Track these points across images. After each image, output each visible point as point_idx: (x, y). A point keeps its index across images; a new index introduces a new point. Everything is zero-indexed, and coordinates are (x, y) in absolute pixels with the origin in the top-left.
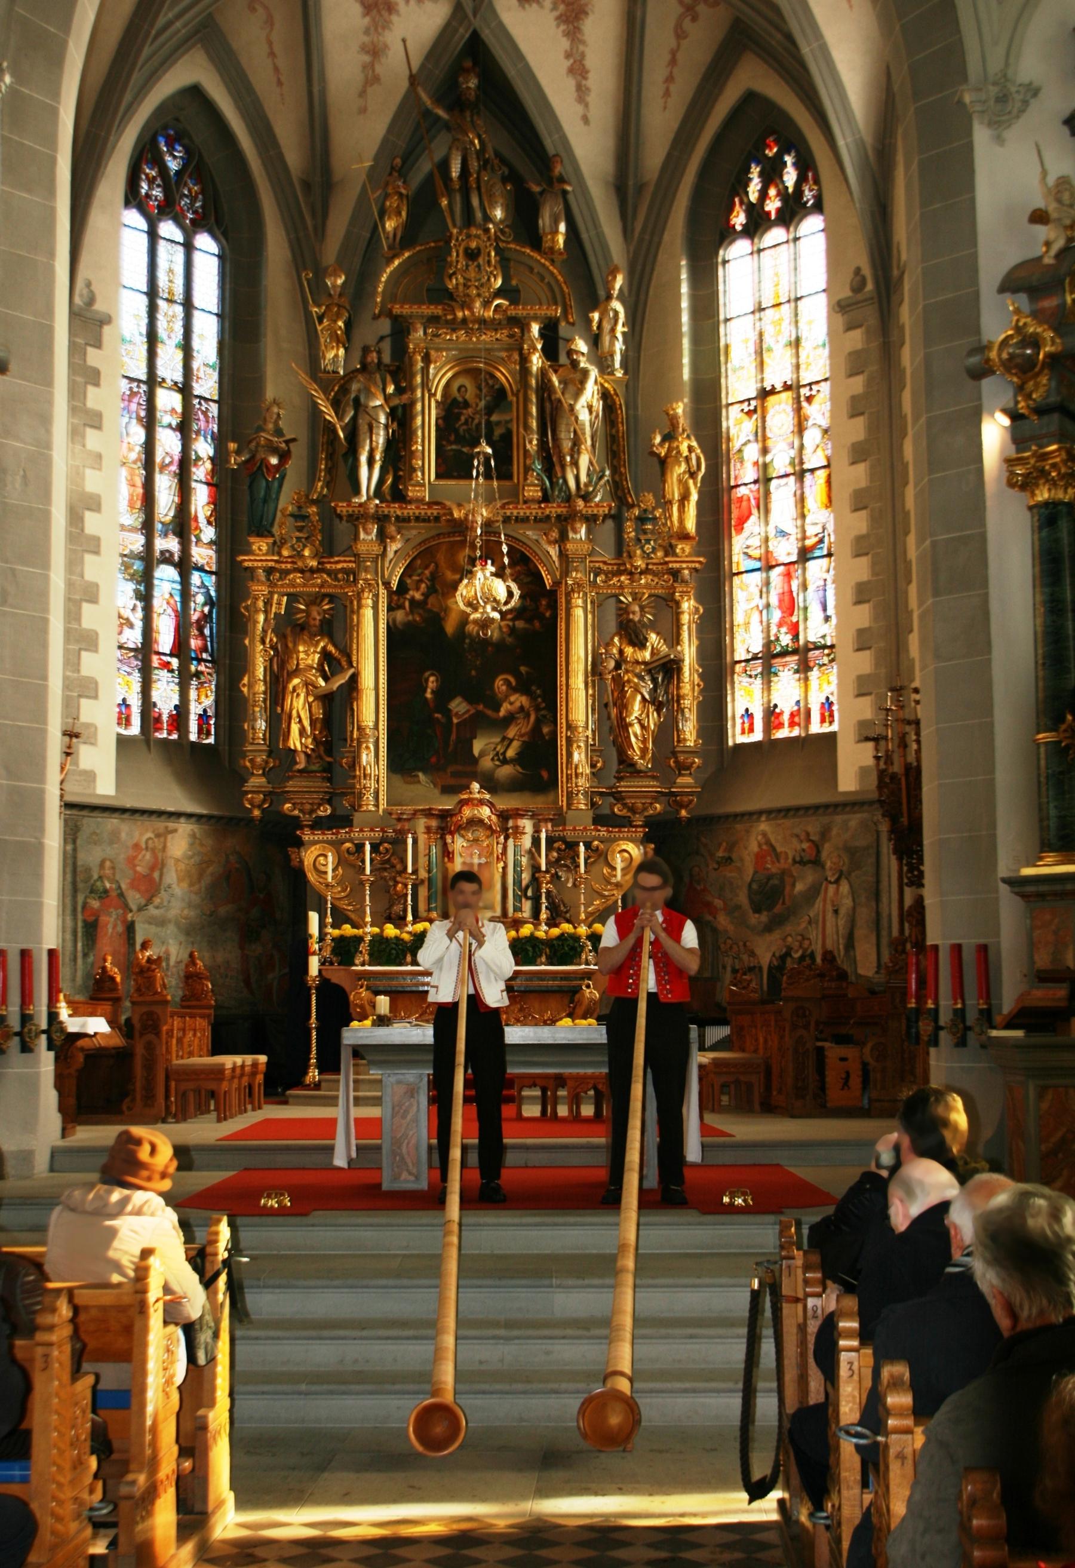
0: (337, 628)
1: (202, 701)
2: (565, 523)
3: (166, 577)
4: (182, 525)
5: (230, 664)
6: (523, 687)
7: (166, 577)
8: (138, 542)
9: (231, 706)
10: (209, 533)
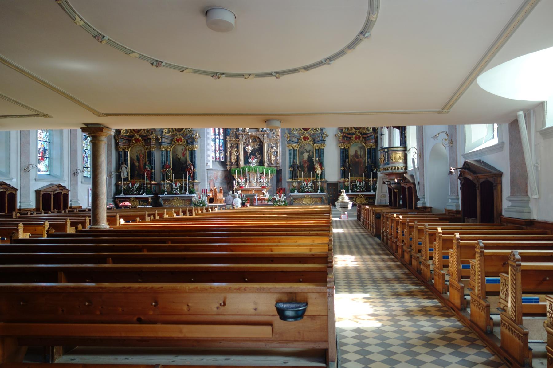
0: (238, 147)
1: (222, 155)
2: (264, 135)
3: (217, 141)
4: (219, 134)
5: (225, 152)
6: (259, 154)
7: (217, 141)
8: (213, 137)
9: (225, 156)
10: (222, 135)
